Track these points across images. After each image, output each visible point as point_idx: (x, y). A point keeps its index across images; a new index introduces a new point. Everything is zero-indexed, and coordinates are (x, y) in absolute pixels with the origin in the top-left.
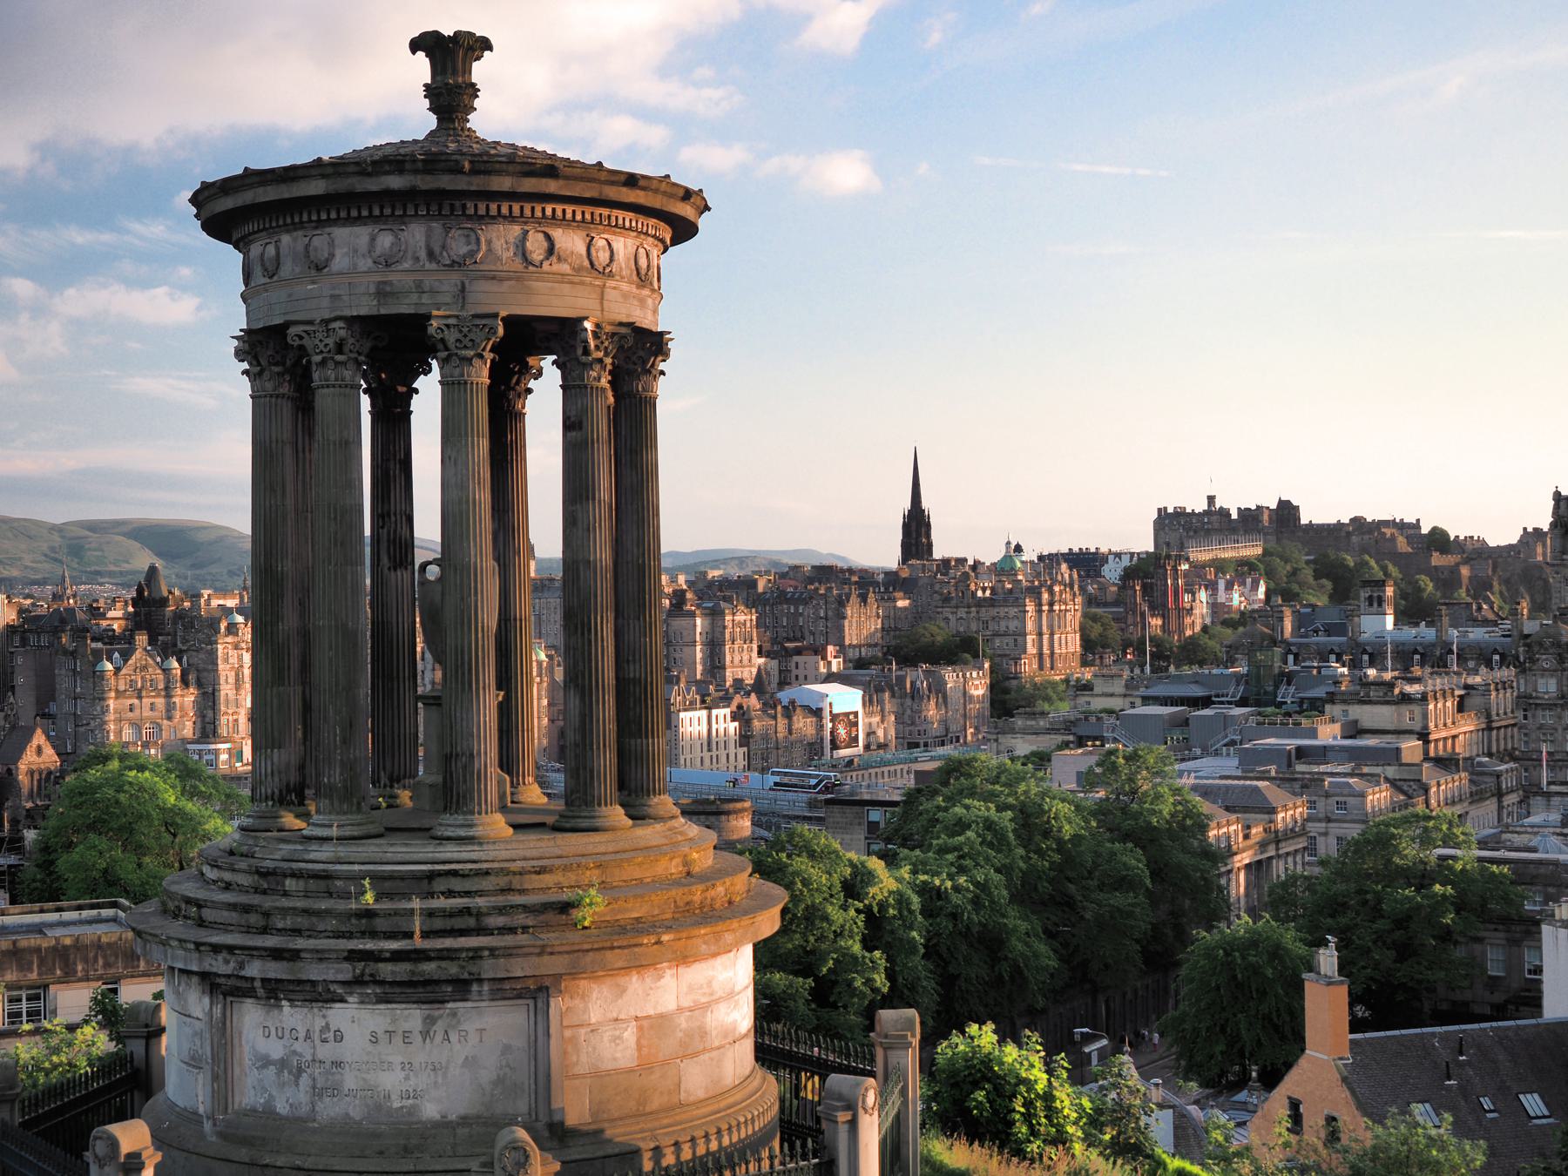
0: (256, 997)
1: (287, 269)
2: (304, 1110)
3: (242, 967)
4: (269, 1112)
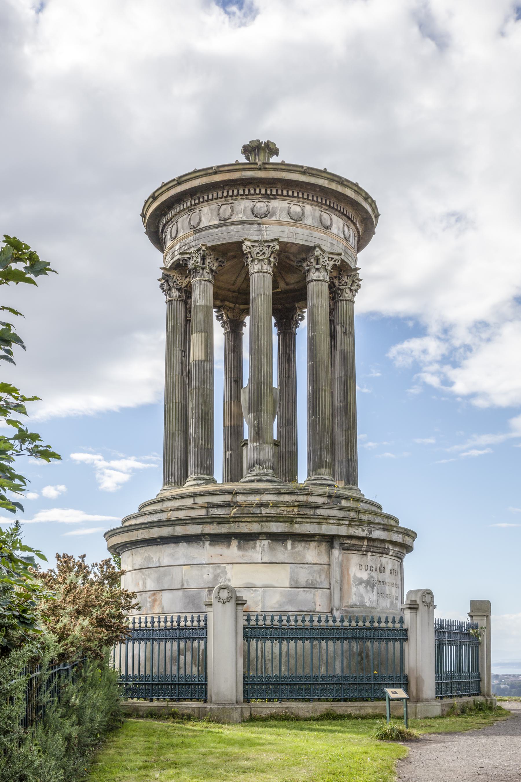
0: (361, 551)
1: (309, 221)
2: (374, 605)
3: (370, 532)
4: (362, 605)
